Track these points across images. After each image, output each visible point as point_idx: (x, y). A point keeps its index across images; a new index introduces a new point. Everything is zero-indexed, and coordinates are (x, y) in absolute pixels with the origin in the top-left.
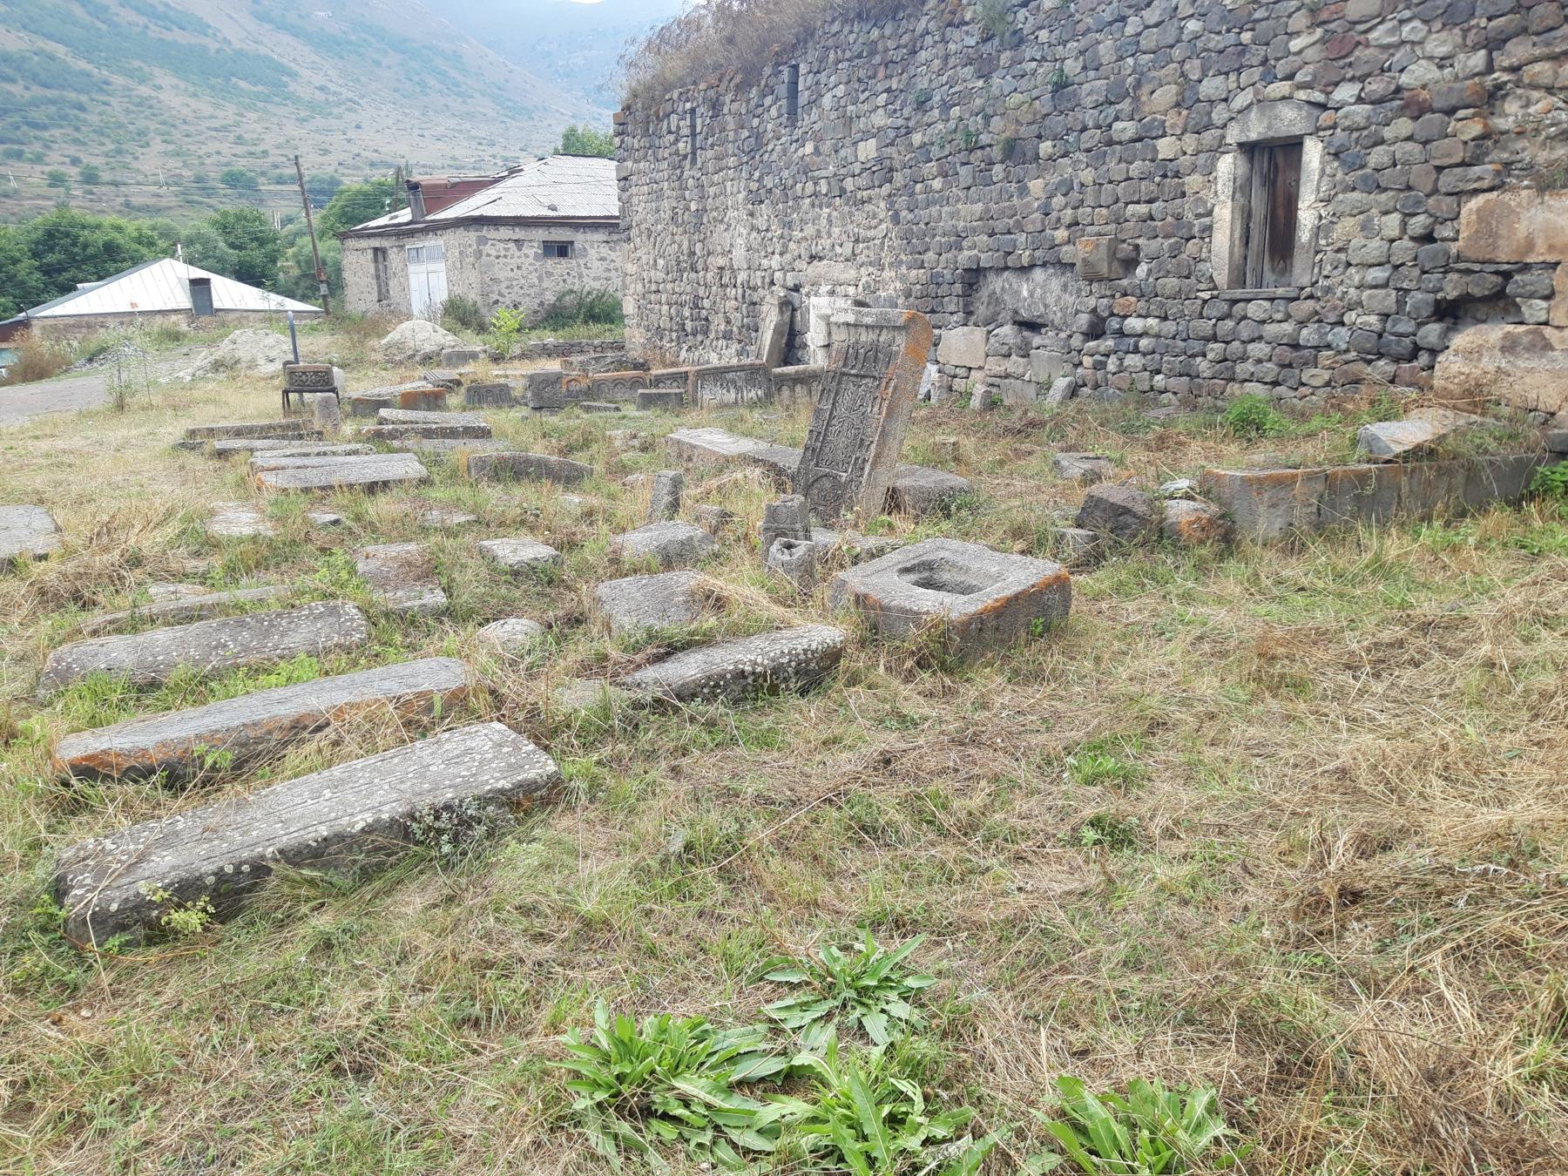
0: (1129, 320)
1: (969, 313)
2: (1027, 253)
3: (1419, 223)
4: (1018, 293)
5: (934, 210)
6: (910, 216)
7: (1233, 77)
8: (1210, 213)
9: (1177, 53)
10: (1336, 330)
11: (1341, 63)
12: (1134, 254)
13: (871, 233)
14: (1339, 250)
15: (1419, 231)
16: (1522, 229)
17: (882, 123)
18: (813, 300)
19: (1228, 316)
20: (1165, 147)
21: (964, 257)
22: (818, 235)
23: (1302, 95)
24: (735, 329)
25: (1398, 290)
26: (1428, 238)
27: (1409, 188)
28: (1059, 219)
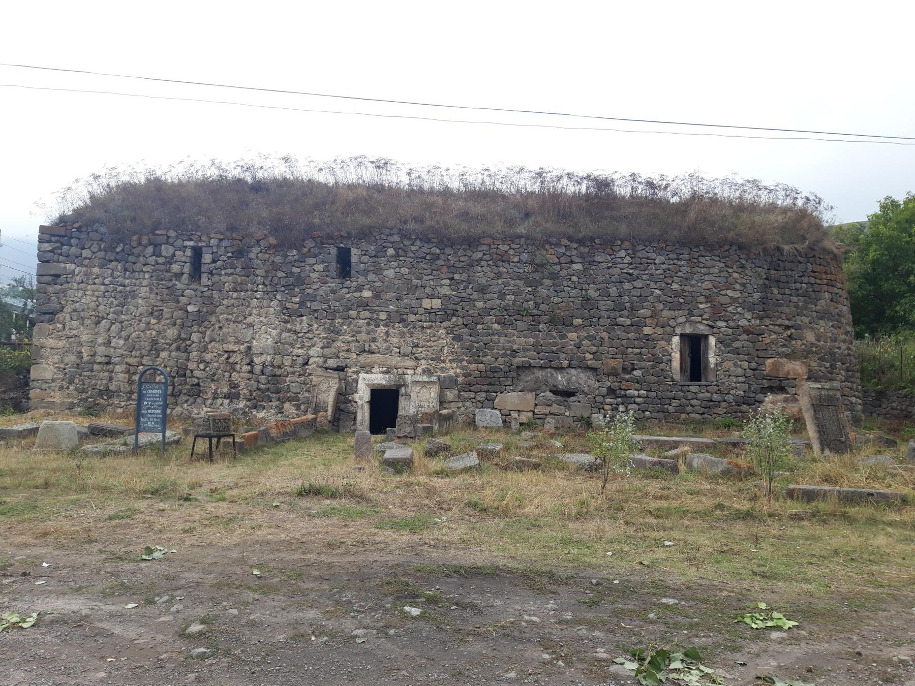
0: (628, 392)
3: (754, 365)
8: (670, 355)
15: (755, 367)
16: (786, 369)
17: (447, 293)
18: (362, 375)
21: (518, 360)
22: (374, 340)
23: (705, 322)
26: (754, 370)
27: (748, 354)
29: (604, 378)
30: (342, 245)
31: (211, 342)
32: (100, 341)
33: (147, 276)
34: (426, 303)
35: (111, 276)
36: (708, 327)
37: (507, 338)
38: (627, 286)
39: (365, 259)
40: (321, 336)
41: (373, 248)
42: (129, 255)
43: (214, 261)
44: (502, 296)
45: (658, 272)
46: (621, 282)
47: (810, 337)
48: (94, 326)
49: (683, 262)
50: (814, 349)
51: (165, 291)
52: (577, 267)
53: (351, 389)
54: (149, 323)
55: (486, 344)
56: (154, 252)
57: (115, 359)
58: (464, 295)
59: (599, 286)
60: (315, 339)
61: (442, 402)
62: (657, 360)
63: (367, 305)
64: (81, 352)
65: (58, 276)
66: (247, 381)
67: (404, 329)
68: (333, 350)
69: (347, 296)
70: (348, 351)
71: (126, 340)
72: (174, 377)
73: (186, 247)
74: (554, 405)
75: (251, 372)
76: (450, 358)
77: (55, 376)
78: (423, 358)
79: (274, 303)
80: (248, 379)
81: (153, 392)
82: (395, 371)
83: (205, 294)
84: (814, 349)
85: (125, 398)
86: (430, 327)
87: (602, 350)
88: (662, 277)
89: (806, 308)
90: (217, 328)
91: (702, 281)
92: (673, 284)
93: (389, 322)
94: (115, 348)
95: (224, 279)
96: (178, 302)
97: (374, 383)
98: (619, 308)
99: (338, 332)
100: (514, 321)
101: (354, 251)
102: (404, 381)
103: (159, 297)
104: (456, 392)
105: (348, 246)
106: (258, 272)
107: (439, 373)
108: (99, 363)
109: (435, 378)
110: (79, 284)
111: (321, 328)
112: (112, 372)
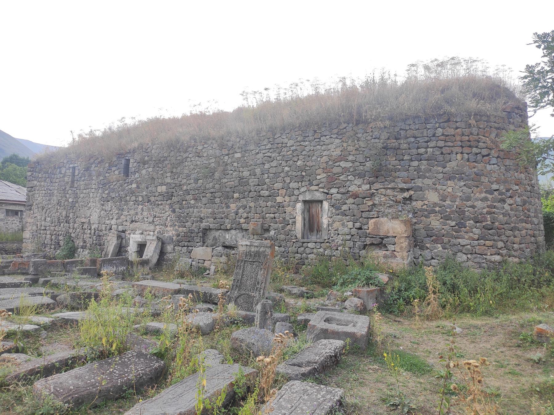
1: (204, 243)
3: (358, 225)
4: (225, 237)
5: (191, 210)
6: (181, 211)
7: (300, 183)
8: (295, 218)
9: (282, 175)
11: (332, 183)
12: (268, 228)
13: (162, 215)
14: (335, 230)
15: (358, 227)
17: (169, 181)
18: (132, 235)
19: (302, 246)
20: (279, 199)
21: (203, 225)
22: (137, 214)
23: (322, 190)
24: (88, 245)
25: (353, 241)
26: (360, 228)
27: (354, 216)
28: (241, 216)
30: (127, 158)
31: (77, 218)
37: (197, 210)
43: (79, 174)
44: (196, 180)
45: (288, 153)
46: (264, 164)
47: (433, 197)
49: (307, 143)
52: (238, 155)
55: (187, 214)
58: (177, 182)
59: (250, 168)
65: (32, 187)
68: (120, 220)
70: (126, 221)
75: (90, 234)
76: (169, 224)
78: (158, 225)
79: (99, 195)
84: (437, 209)
86: (162, 204)
91: (322, 156)
95: (82, 183)
96: (66, 197)
98: (261, 183)
99: (122, 210)
100: (201, 198)
101: (131, 161)
103: (60, 195)
105: (130, 158)
111: (115, 208)
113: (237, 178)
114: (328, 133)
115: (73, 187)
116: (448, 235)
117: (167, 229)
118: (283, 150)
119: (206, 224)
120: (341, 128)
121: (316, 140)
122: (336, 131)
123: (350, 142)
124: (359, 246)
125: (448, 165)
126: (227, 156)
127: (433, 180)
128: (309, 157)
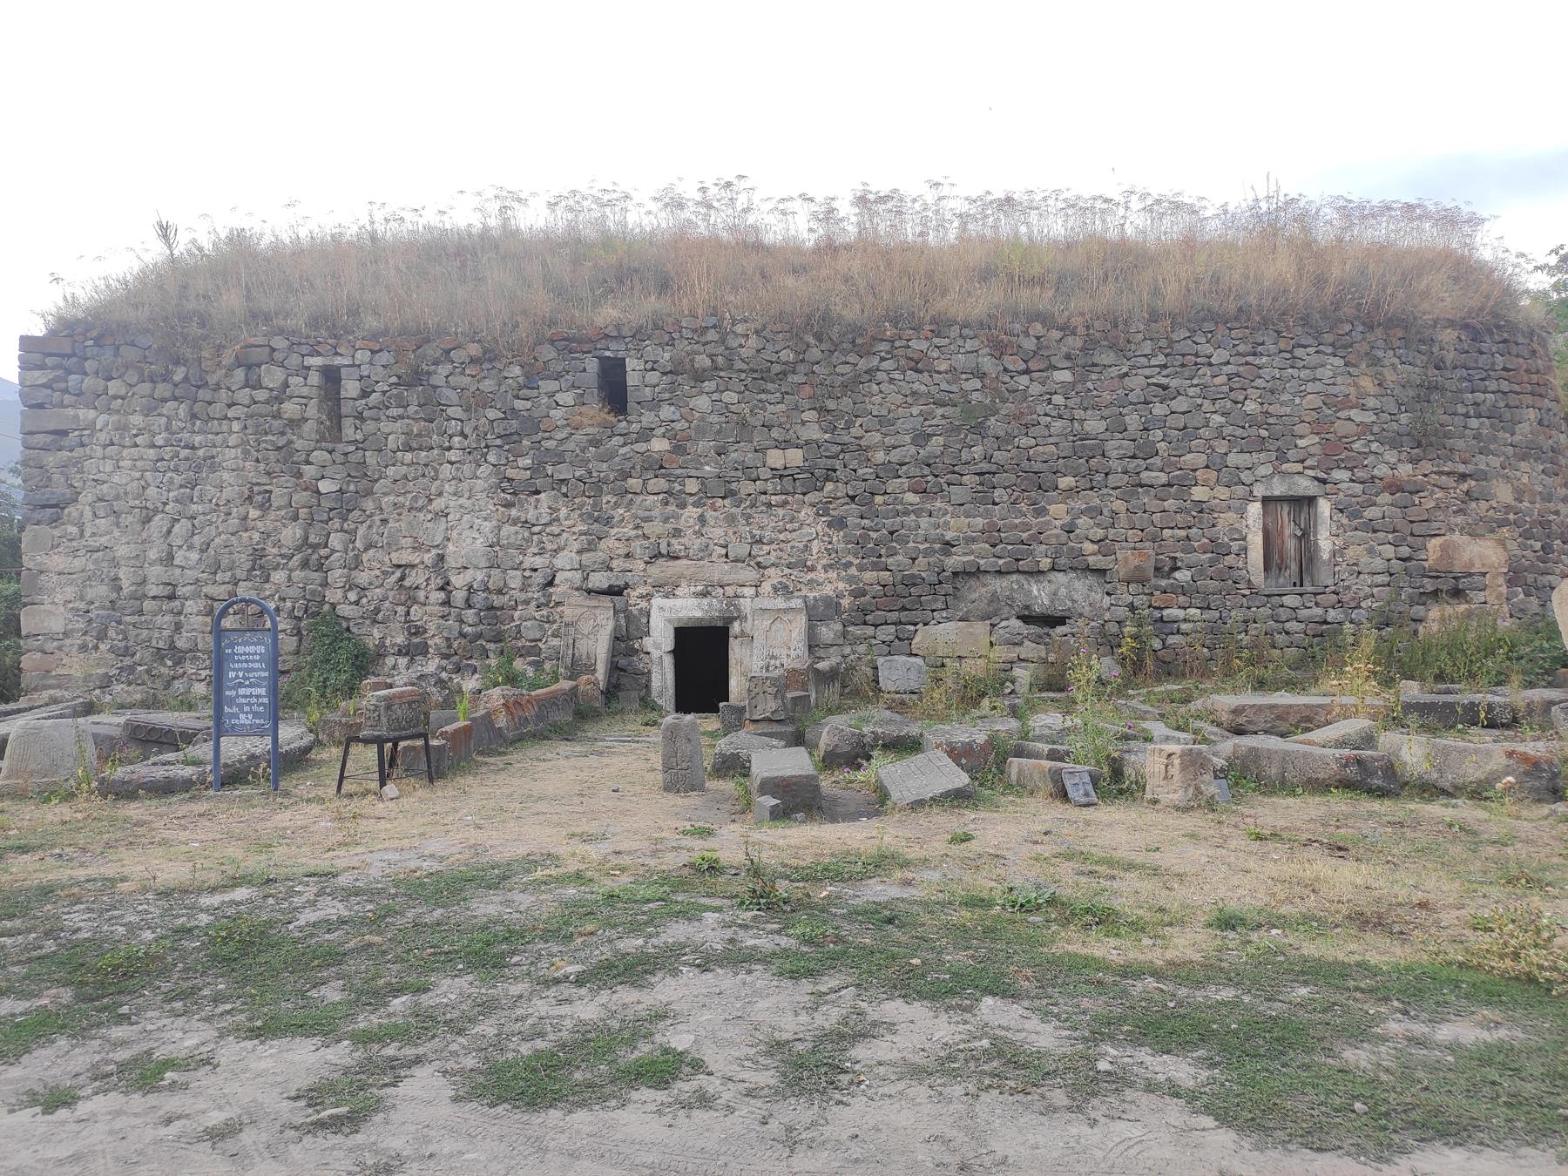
0: (1165, 612)
2: (1049, 560)
3: (1405, 551)
4: (1030, 592)
8: (1244, 539)
10: (1356, 611)
15: (1407, 555)
18: (657, 601)
20: (1198, 493)
21: (955, 561)
22: (677, 533)
24: (435, 642)
26: (1408, 559)
27: (1394, 531)
29: (1121, 588)
30: (608, 354)
31: (366, 549)
32: (153, 554)
33: (236, 426)
34: (775, 458)
35: (167, 429)
36: (1316, 483)
37: (932, 520)
38: (1159, 409)
39: (653, 377)
40: (575, 530)
41: (667, 356)
42: (199, 387)
43: (365, 394)
44: (921, 438)
45: (1217, 381)
46: (1146, 403)
47: (1504, 493)
48: (138, 527)
49: (1264, 360)
50: (1511, 517)
51: (272, 456)
53: (638, 629)
54: (245, 518)
55: (892, 533)
56: (247, 380)
57: (184, 589)
58: (846, 439)
59: (1106, 412)
60: (565, 535)
61: (813, 646)
62: (1218, 549)
63: (662, 467)
64: (117, 579)
65: (64, 433)
66: (441, 621)
67: (733, 510)
68: (600, 556)
69: (622, 451)
70: (627, 556)
71: (202, 551)
72: (299, 619)
73: (308, 368)
74: (1027, 643)
75: (447, 603)
76: (824, 562)
77: (70, 627)
78: (773, 565)
79: (485, 470)
80: (442, 617)
81: (247, 649)
82: (720, 591)
83: (352, 458)
84: (1511, 517)
85: (208, 662)
86: (786, 503)
87: (1115, 534)
88: (1226, 389)
89: (1495, 439)
90: (378, 523)
91: (1303, 394)
92: (1247, 402)
93: (705, 496)
94: (183, 568)
95: (386, 426)
96: (299, 475)
97: (681, 615)
99: (608, 521)
100: (945, 486)
101: (631, 364)
102: (739, 610)
103: (262, 466)
104: (839, 627)
105: (620, 355)
106: (450, 411)
107: (804, 592)
108: (154, 598)
109: (800, 601)
110: (105, 446)
112: (180, 613)
113: (1066, 435)
114: (1310, 341)
115: (340, 441)
116: (1531, 568)
117: (810, 576)
118: (1200, 372)
119: (966, 559)
120: (1340, 332)
121: (1282, 355)
122: (1329, 338)
123: (1363, 366)
124: (1411, 597)
125: (1518, 428)
126: (1026, 377)
127: (1502, 459)
128: (1273, 393)
